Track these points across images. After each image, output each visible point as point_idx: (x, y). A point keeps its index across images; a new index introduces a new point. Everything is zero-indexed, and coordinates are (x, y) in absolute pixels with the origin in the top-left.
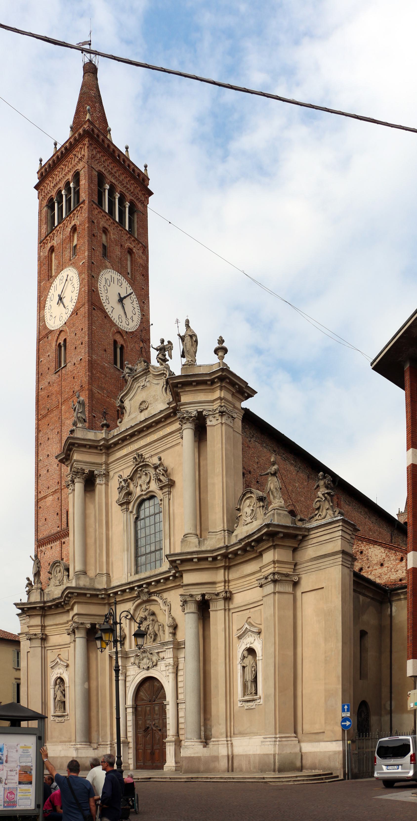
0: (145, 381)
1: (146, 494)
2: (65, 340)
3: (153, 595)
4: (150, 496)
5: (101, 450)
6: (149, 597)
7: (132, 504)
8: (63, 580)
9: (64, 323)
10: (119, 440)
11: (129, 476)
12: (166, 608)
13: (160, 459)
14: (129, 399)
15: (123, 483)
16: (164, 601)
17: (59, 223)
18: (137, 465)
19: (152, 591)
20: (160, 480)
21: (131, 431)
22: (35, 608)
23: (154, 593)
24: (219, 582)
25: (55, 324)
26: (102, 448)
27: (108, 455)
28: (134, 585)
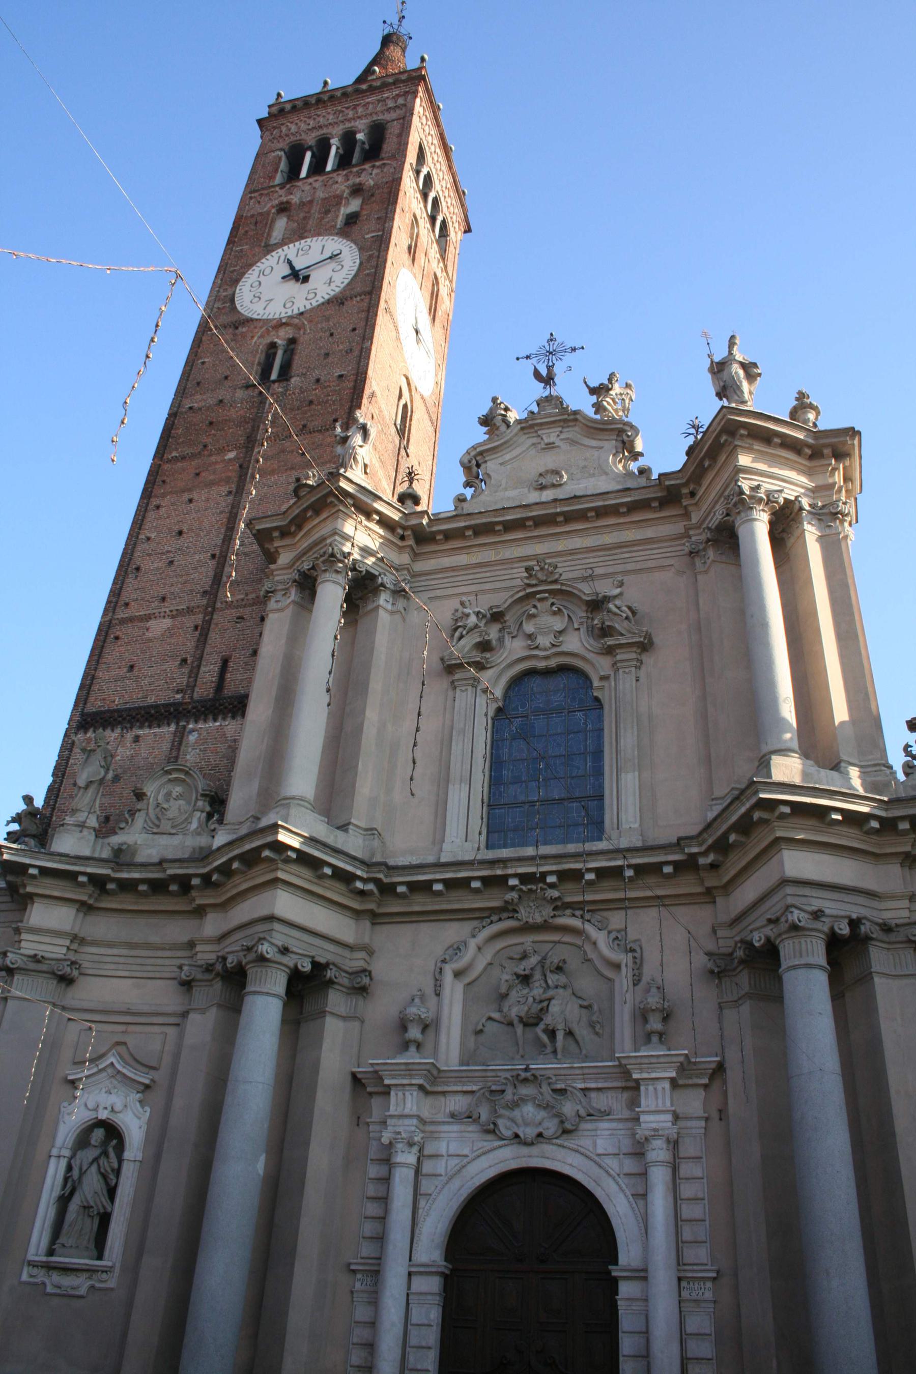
0: (558, 436)
1: (546, 658)
2: (292, 341)
3: (568, 912)
4: (558, 666)
5: (402, 538)
6: (554, 916)
7: (489, 673)
8: (188, 821)
9: (296, 312)
10: (467, 528)
11: (497, 606)
12: (624, 959)
13: (621, 584)
14: (500, 460)
15: (473, 620)
16: (613, 935)
17: (308, 176)
18: (529, 585)
19: (568, 899)
20: (605, 632)
21: (518, 516)
22: (71, 876)
23: (574, 909)
24: (893, 897)
25: (267, 312)
26: (409, 533)
27: (415, 556)
28: (510, 871)
